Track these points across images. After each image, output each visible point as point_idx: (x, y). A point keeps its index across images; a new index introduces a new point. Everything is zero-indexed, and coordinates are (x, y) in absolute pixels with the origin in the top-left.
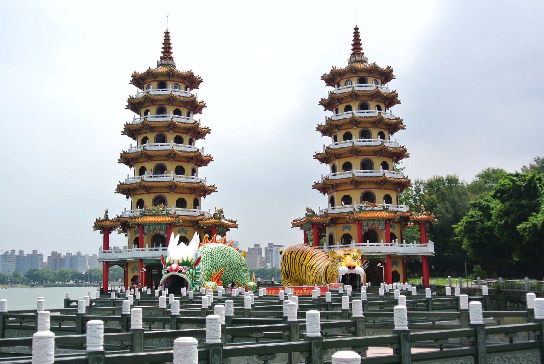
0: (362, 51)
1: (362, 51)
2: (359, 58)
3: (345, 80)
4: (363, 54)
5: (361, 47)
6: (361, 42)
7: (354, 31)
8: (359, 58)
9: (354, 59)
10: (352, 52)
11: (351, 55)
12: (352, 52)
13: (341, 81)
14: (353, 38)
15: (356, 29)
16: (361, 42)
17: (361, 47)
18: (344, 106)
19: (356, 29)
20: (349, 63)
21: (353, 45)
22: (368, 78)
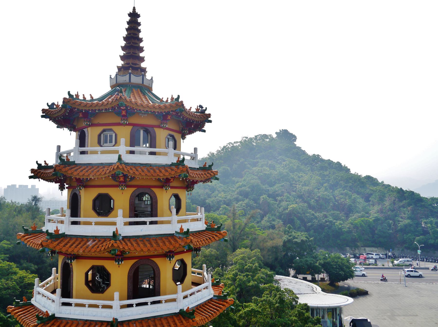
0: (143, 65)
1: (143, 65)
2: (136, 80)
3: (100, 129)
4: (144, 70)
5: (141, 55)
6: (141, 45)
7: (128, 18)
8: (136, 80)
9: (125, 79)
10: (120, 63)
11: (119, 69)
12: (120, 63)
13: (89, 129)
14: (125, 33)
15: (134, 16)
16: (141, 45)
17: (141, 55)
18: (93, 193)
19: (134, 16)
20: (112, 87)
21: (123, 48)
22: (157, 130)
